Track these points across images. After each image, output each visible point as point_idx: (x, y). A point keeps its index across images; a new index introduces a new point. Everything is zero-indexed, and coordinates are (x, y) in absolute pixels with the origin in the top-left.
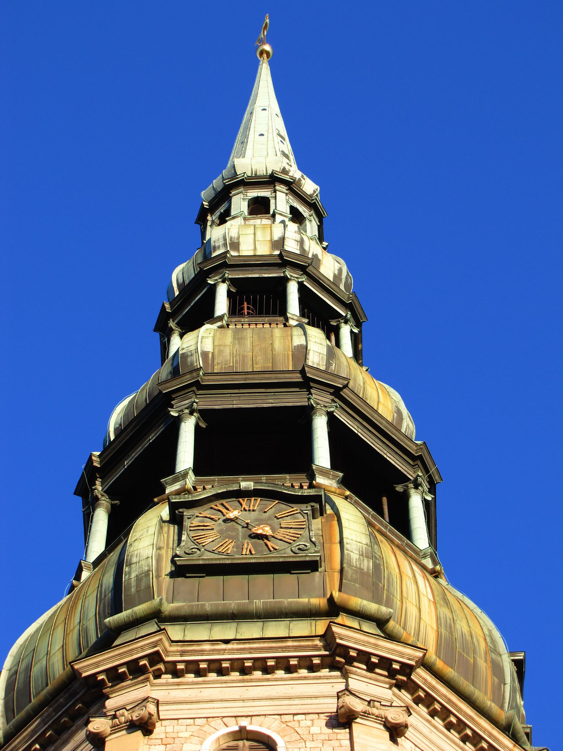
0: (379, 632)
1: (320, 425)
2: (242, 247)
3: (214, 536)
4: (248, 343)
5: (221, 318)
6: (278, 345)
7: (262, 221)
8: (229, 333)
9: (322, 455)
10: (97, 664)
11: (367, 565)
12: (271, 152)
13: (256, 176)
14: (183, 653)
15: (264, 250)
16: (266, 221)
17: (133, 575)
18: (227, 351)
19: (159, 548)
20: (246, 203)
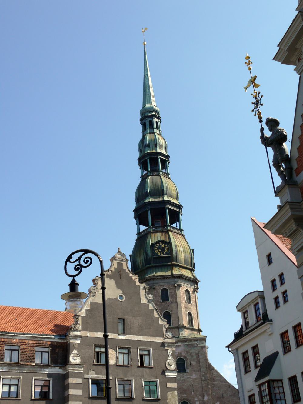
17: (148, 258)
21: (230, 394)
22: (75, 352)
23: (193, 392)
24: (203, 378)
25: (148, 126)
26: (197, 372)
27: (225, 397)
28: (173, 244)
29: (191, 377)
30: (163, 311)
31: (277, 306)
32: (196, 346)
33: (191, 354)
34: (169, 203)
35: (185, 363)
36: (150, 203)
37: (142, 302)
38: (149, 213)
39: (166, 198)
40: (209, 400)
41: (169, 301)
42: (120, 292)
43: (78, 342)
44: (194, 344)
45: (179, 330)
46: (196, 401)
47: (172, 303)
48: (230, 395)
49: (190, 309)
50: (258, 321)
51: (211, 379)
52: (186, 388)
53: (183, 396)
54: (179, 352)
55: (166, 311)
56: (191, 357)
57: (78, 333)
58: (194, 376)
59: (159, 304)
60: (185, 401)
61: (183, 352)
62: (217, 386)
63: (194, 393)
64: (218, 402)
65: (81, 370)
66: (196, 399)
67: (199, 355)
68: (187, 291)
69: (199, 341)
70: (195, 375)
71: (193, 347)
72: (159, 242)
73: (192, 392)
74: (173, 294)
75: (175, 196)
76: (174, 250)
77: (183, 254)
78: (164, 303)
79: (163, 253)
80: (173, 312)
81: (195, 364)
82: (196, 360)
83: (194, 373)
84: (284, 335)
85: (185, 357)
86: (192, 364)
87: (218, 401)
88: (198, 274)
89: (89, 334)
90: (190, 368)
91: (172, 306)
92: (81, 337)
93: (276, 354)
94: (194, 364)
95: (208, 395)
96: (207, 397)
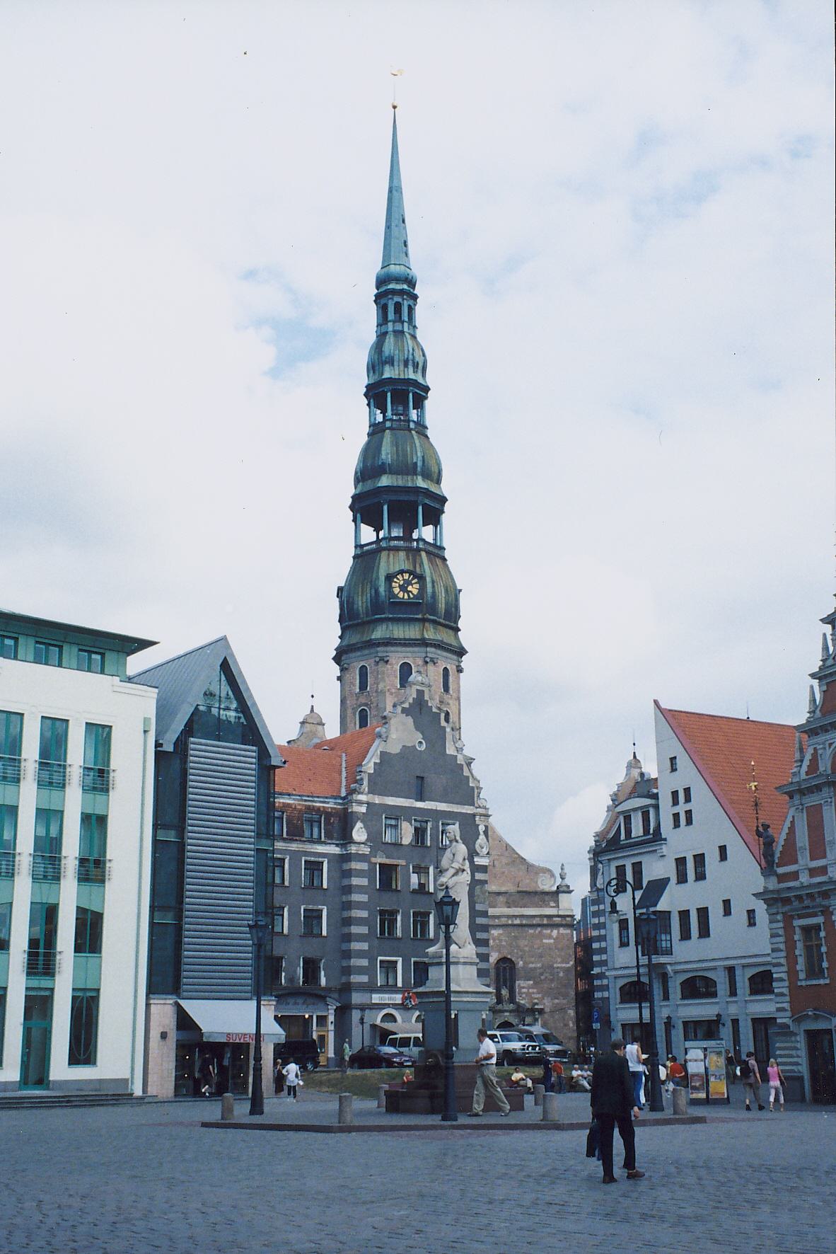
1: (420, 509)
22: (359, 825)
25: (391, 316)
28: (428, 579)
31: (677, 824)
34: (427, 493)
36: (388, 489)
37: (448, 752)
38: (385, 507)
39: (421, 483)
42: (419, 737)
43: (363, 809)
50: (646, 831)
57: (363, 798)
65: (366, 850)
68: (446, 670)
72: (402, 572)
75: (435, 476)
76: (429, 590)
84: (681, 862)
88: (465, 638)
89: (377, 800)
92: (368, 803)
93: (668, 880)
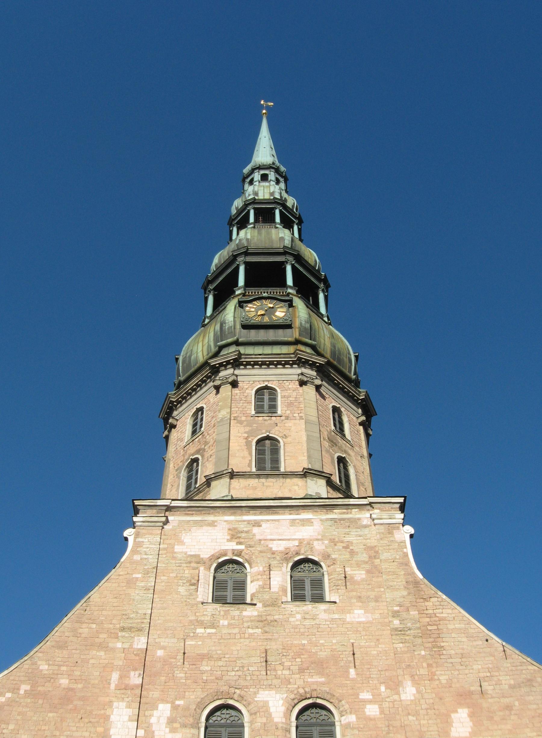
0: (313, 353)
2: (259, 195)
3: (253, 311)
4: (263, 235)
5: (251, 224)
6: (274, 236)
7: (266, 184)
8: (256, 231)
9: (290, 281)
10: (216, 361)
11: (308, 326)
12: (268, 155)
13: (264, 165)
14: (245, 358)
15: (267, 197)
16: (267, 184)
17: (227, 327)
18: (256, 239)
19: (234, 317)
20: (260, 176)
21: (512, 682)
23: (352, 671)
24: (396, 622)
26: (373, 604)
27: (490, 692)
29: (349, 618)
30: (256, 437)
32: (366, 526)
33: (346, 547)
35: (325, 573)
40: (422, 701)
41: (279, 412)
44: (359, 519)
45: (306, 482)
46: (366, 702)
47: (287, 418)
48: (512, 687)
49: (345, 452)
51: (429, 628)
52: (323, 654)
53: (309, 680)
54: (303, 539)
55: (268, 438)
56: (348, 556)
58: (358, 615)
59: (243, 418)
60: (319, 701)
61: (317, 540)
62: (453, 652)
63: (357, 674)
64: (460, 710)
66: (365, 695)
67: (377, 552)
69: (376, 511)
70: (362, 611)
71: (357, 528)
73: (350, 667)
74: (291, 399)
77: (326, 337)
78: (261, 418)
79: (270, 318)
80: (289, 439)
81: (364, 576)
82: (367, 567)
83: (360, 604)
85: (327, 556)
86: (352, 578)
87: (461, 705)
90: (344, 588)
91: (286, 425)
94: (358, 578)
95: (415, 683)
96: (414, 690)
